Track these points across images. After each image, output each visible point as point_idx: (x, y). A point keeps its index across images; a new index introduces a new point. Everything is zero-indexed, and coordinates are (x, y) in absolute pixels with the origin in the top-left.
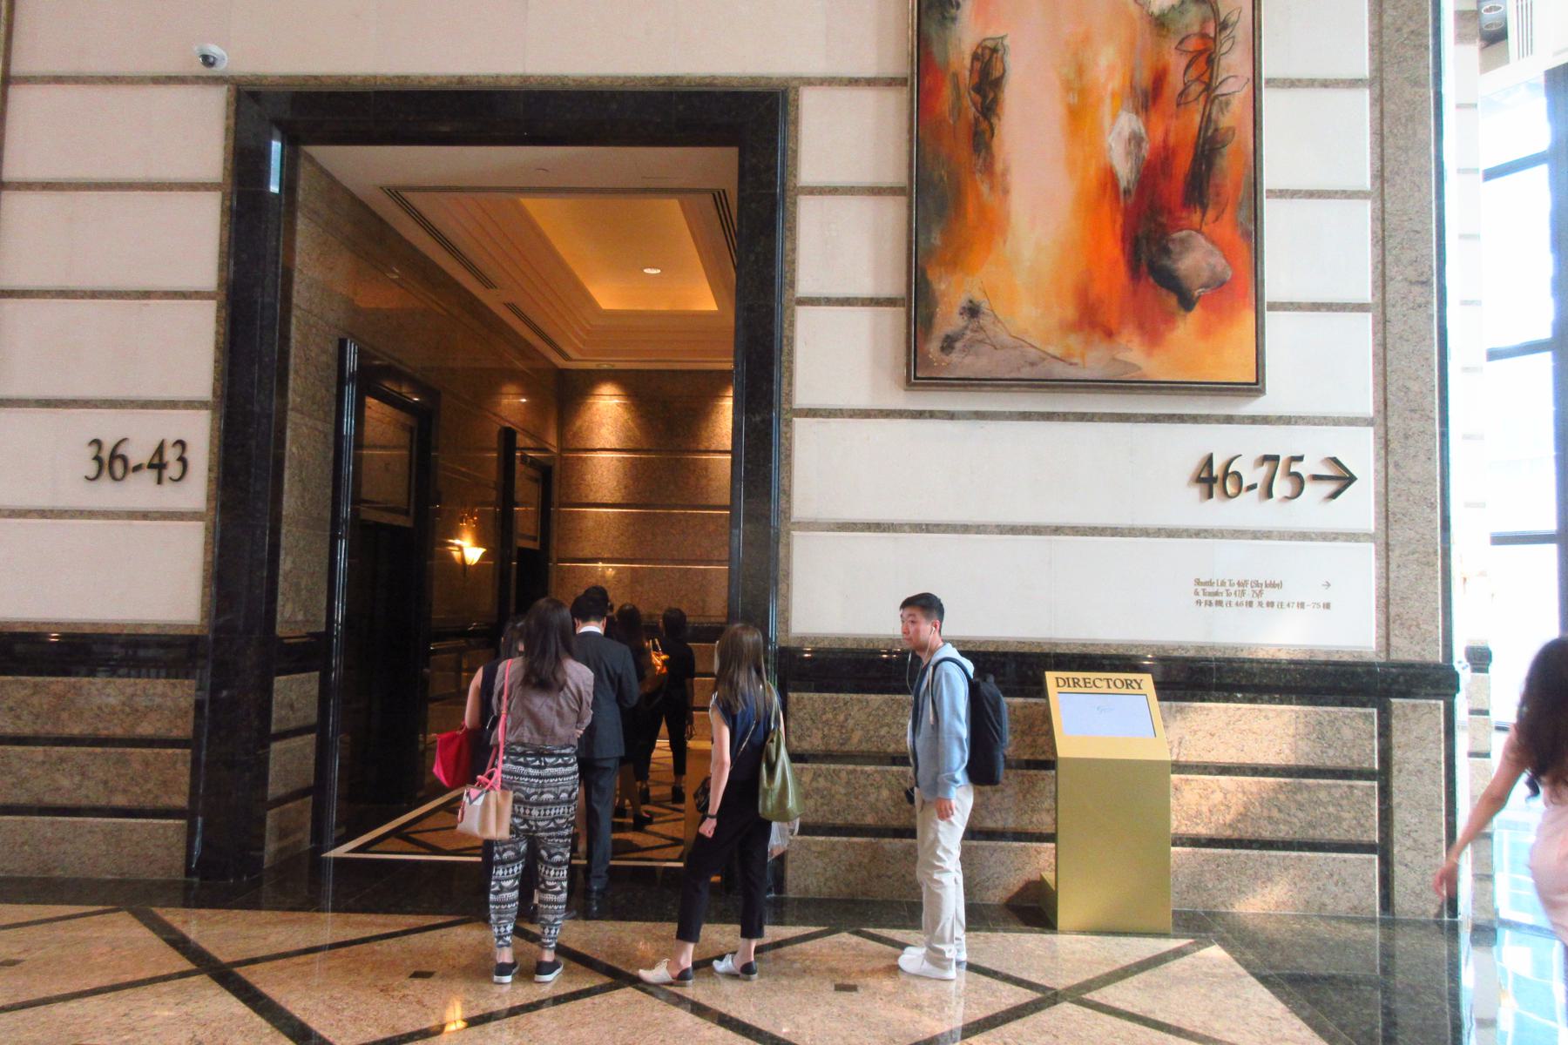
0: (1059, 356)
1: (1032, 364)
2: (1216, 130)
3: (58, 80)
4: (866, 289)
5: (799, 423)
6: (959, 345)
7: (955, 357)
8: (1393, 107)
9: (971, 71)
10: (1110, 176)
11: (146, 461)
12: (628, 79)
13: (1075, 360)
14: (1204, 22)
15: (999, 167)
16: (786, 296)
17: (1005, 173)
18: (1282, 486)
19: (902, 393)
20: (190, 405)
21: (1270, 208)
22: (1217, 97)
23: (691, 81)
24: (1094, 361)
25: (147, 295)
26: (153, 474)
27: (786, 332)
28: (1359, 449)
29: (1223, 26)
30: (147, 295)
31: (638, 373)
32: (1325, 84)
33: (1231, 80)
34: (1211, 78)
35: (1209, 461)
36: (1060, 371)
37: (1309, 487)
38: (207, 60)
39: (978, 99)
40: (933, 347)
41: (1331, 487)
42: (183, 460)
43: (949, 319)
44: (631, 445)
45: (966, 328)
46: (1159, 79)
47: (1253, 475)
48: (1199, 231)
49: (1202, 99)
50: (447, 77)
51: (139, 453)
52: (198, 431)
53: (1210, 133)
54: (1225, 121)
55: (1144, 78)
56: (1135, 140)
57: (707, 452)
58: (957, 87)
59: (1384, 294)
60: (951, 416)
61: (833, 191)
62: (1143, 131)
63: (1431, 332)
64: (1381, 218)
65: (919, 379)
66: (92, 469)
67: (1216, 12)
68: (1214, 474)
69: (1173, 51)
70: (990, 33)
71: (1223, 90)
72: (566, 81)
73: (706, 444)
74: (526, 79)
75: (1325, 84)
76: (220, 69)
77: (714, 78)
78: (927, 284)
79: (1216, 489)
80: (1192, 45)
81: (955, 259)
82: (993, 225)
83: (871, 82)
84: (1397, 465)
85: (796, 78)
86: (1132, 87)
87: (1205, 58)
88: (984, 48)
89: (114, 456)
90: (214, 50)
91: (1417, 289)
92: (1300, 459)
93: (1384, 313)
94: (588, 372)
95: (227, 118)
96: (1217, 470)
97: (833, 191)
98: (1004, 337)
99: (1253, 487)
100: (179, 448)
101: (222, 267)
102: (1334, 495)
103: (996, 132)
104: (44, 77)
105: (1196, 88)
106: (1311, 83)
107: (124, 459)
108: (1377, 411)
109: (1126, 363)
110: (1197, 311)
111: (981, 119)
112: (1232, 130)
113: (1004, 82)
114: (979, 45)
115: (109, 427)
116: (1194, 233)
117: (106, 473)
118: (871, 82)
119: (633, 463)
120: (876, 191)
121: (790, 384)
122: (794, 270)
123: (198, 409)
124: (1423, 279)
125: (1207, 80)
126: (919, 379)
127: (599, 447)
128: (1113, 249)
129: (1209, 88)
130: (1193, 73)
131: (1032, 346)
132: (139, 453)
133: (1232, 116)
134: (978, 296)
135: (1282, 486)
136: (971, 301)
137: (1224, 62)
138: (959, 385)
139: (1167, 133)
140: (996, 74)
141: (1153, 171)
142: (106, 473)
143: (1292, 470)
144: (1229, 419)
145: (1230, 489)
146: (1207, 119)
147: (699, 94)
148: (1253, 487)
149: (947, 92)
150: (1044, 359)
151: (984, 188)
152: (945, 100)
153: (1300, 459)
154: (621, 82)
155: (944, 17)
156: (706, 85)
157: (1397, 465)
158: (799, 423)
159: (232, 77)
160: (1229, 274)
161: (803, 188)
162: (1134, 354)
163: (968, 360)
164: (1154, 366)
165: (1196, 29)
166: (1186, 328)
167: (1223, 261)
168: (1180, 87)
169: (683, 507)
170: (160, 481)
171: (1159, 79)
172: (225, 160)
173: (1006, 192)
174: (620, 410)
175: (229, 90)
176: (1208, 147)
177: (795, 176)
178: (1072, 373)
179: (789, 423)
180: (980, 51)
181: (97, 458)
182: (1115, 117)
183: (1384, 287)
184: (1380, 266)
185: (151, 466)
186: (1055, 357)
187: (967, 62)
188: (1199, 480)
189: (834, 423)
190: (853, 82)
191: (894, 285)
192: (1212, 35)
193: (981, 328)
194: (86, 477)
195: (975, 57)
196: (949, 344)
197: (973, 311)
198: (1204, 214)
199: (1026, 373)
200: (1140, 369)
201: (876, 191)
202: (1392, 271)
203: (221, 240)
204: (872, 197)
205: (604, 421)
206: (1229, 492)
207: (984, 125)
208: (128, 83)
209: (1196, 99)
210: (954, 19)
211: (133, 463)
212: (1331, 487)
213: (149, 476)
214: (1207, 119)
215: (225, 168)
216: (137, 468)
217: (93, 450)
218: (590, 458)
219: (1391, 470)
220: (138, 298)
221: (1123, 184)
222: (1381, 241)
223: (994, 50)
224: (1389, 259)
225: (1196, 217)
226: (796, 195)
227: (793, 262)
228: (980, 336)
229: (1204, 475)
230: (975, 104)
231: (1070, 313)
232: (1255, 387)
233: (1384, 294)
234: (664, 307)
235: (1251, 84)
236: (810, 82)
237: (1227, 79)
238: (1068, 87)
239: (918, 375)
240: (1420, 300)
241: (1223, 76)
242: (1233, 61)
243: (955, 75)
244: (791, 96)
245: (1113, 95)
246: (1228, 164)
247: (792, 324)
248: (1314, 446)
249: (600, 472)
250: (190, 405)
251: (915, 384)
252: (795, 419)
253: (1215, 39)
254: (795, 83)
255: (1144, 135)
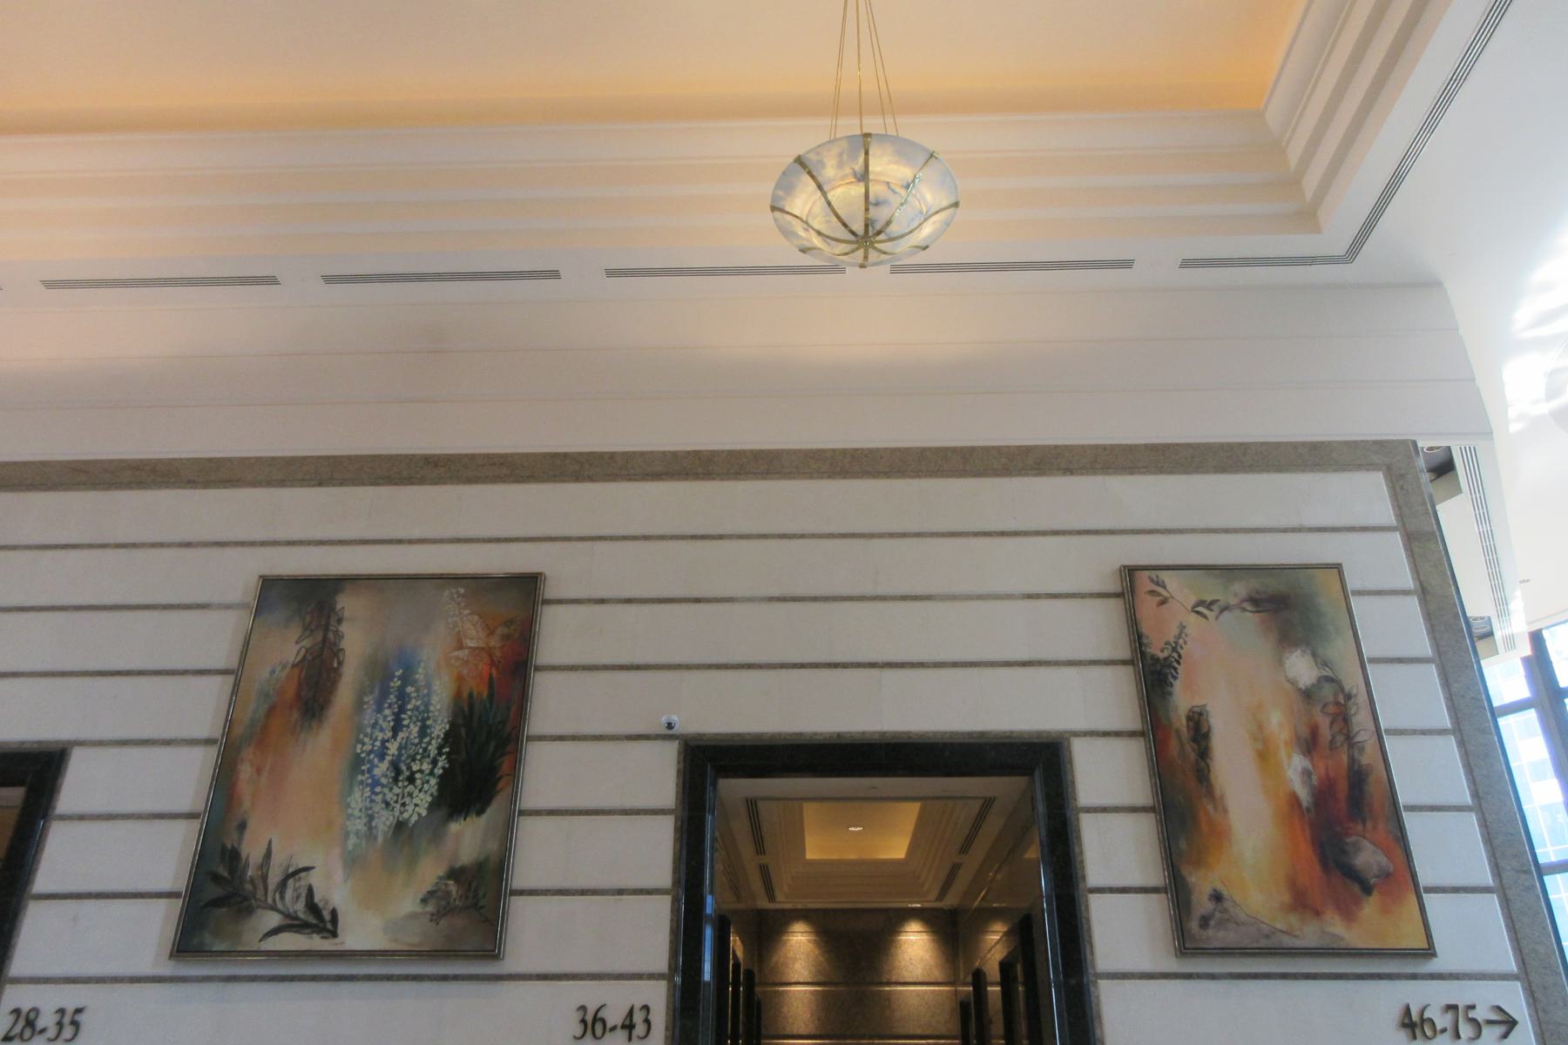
0: (1284, 930)
1: (1267, 937)
2: (1360, 766)
3: (561, 738)
4: (1136, 880)
5: (1102, 983)
6: (1212, 923)
7: (1210, 932)
8: (1473, 748)
9: (1188, 726)
10: (1294, 800)
11: (620, 1024)
12: (953, 734)
13: (1297, 933)
14: (1336, 695)
15: (1218, 793)
16: (1081, 886)
17: (1222, 797)
18: (1466, 1030)
19: (1175, 959)
20: (651, 976)
21: (1407, 817)
22: (1355, 743)
23: (996, 735)
24: (1309, 934)
25: (620, 892)
26: (625, 1033)
27: (1084, 914)
28: (1515, 1000)
29: (1348, 697)
30: (620, 892)
31: (825, 911)
32: (1424, 732)
33: (1362, 732)
34: (1348, 731)
35: (1407, 1011)
36: (1288, 941)
37: (1486, 1031)
38: (670, 726)
39: (1195, 746)
40: (1194, 925)
41: (1501, 1030)
42: (647, 1022)
43: (1202, 903)
44: (822, 979)
45: (1215, 910)
46: (1314, 731)
47: (1442, 1021)
48: (1364, 837)
49: (1346, 747)
50: (829, 733)
51: (614, 1017)
52: (657, 997)
53: (1356, 768)
54: (1365, 760)
55: (1304, 732)
56: (1306, 774)
57: (889, 983)
58: (1179, 737)
59: (1501, 881)
60: (1212, 977)
61: (1104, 810)
62: (1310, 767)
63: (1542, 908)
64: (1484, 824)
65: (1189, 949)
66: (579, 1030)
67: (1342, 689)
68: (1414, 1019)
69: (1320, 714)
70: (1196, 703)
71: (1358, 739)
72: (911, 735)
73: (887, 977)
74: (883, 734)
75: (1424, 732)
76: (677, 730)
77: (1012, 732)
78: (1183, 879)
79: (1418, 1032)
80: (1331, 709)
81: (1199, 862)
82: (1220, 834)
83: (1117, 734)
84: (1544, 1011)
85: (1067, 732)
86: (1298, 738)
87: (1342, 717)
88: (1194, 712)
89: (595, 1019)
90: (675, 718)
91: (1523, 876)
92: (1473, 1007)
93: (1505, 895)
94: (783, 911)
95: (679, 763)
96: (1415, 1017)
97: (1104, 810)
98: (1243, 917)
99: (1444, 1030)
100: (644, 1012)
101: (676, 870)
102: (1505, 1036)
103: (1211, 769)
104: (552, 736)
105: (1340, 738)
106: (1414, 732)
107: (603, 1021)
108: (1519, 968)
109: (1334, 935)
110: (1375, 893)
111: (1199, 760)
112: (1369, 765)
113: (1211, 735)
114: (1190, 711)
115: (591, 995)
116: (1362, 839)
117: (589, 1031)
118: (1117, 734)
119: (824, 995)
120: (1133, 809)
121: (1092, 953)
122: (1084, 867)
123: (657, 980)
124: (1525, 868)
125: (1346, 732)
126: (1189, 949)
127: (793, 981)
128: (1307, 851)
129: (1349, 738)
130: (1336, 728)
131: (1265, 923)
132: (614, 1017)
133: (1368, 757)
134: (1220, 888)
135: (1466, 1030)
136: (1215, 890)
137: (1355, 720)
138: (1217, 954)
139: (1327, 769)
140: (1205, 730)
141: (1323, 794)
142: (589, 1031)
143: (1470, 1016)
144: (1414, 977)
145: (1429, 1032)
146: (1352, 760)
147: (1004, 745)
148: (1444, 1030)
149: (1174, 744)
150: (1273, 933)
151: (1210, 808)
152: (1174, 746)
153: (1473, 1007)
154: (947, 736)
155: (1164, 693)
156: (1006, 737)
157: (1544, 1011)
158: (1102, 983)
159: (682, 735)
160: (1392, 869)
161: (1083, 808)
162: (1336, 927)
163: (1221, 934)
164: (1353, 937)
165: (1331, 699)
166: (1370, 908)
167: (1385, 859)
168: (1329, 738)
169: (871, 1037)
170: (630, 1039)
171: (1314, 731)
172: (677, 793)
173: (1225, 811)
174: (811, 946)
175: (679, 744)
176: (1358, 778)
177: (1076, 800)
178: (1298, 943)
179: (1095, 983)
180: (1191, 714)
181: (583, 1021)
182: (1290, 757)
183: (1500, 875)
184: (1493, 859)
185: (623, 1027)
186: (1281, 931)
187: (1184, 721)
188: (1404, 1025)
189: (1128, 983)
190: (1106, 734)
191: (1154, 874)
192: (1342, 702)
193: (1226, 911)
194: (575, 1038)
195: (1189, 718)
196: (1205, 922)
197: (1217, 897)
198: (1364, 824)
199: (1263, 943)
200: (1342, 939)
201: (1133, 809)
202: (1502, 863)
203: (674, 849)
204: (1130, 814)
205: (798, 957)
206: (1428, 1034)
207: (1202, 764)
208: (609, 740)
209: (1342, 745)
210: (1170, 694)
211: (609, 1025)
212: (1501, 1030)
213: (621, 1035)
214: (1352, 760)
215: (677, 799)
216: (613, 1029)
217: (579, 1015)
218: (787, 992)
219: (1541, 1014)
220: (614, 895)
221: (1305, 804)
222: (1489, 840)
223: (1201, 714)
224: (1498, 855)
225: (1360, 827)
226: (1078, 813)
227: (1082, 862)
228: (1226, 916)
229: (1407, 1021)
230: (1193, 750)
231: (1286, 897)
232: (1429, 952)
233: (1501, 881)
234: (852, 856)
235: (1375, 734)
236: (1077, 734)
237: (1359, 731)
238: (1255, 739)
239: (1187, 946)
240: (1527, 884)
241: (1355, 731)
242: (1361, 719)
243: (1178, 731)
244: (1066, 743)
245: (1286, 743)
246: (1373, 789)
247: (1087, 907)
248: (1484, 998)
249: (795, 1004)
250: (651, 976)
251: (1186, 953)
252: (1099, 981)
253: (1345, 705)
254: (1067, 735)
255: (1313, 771)
